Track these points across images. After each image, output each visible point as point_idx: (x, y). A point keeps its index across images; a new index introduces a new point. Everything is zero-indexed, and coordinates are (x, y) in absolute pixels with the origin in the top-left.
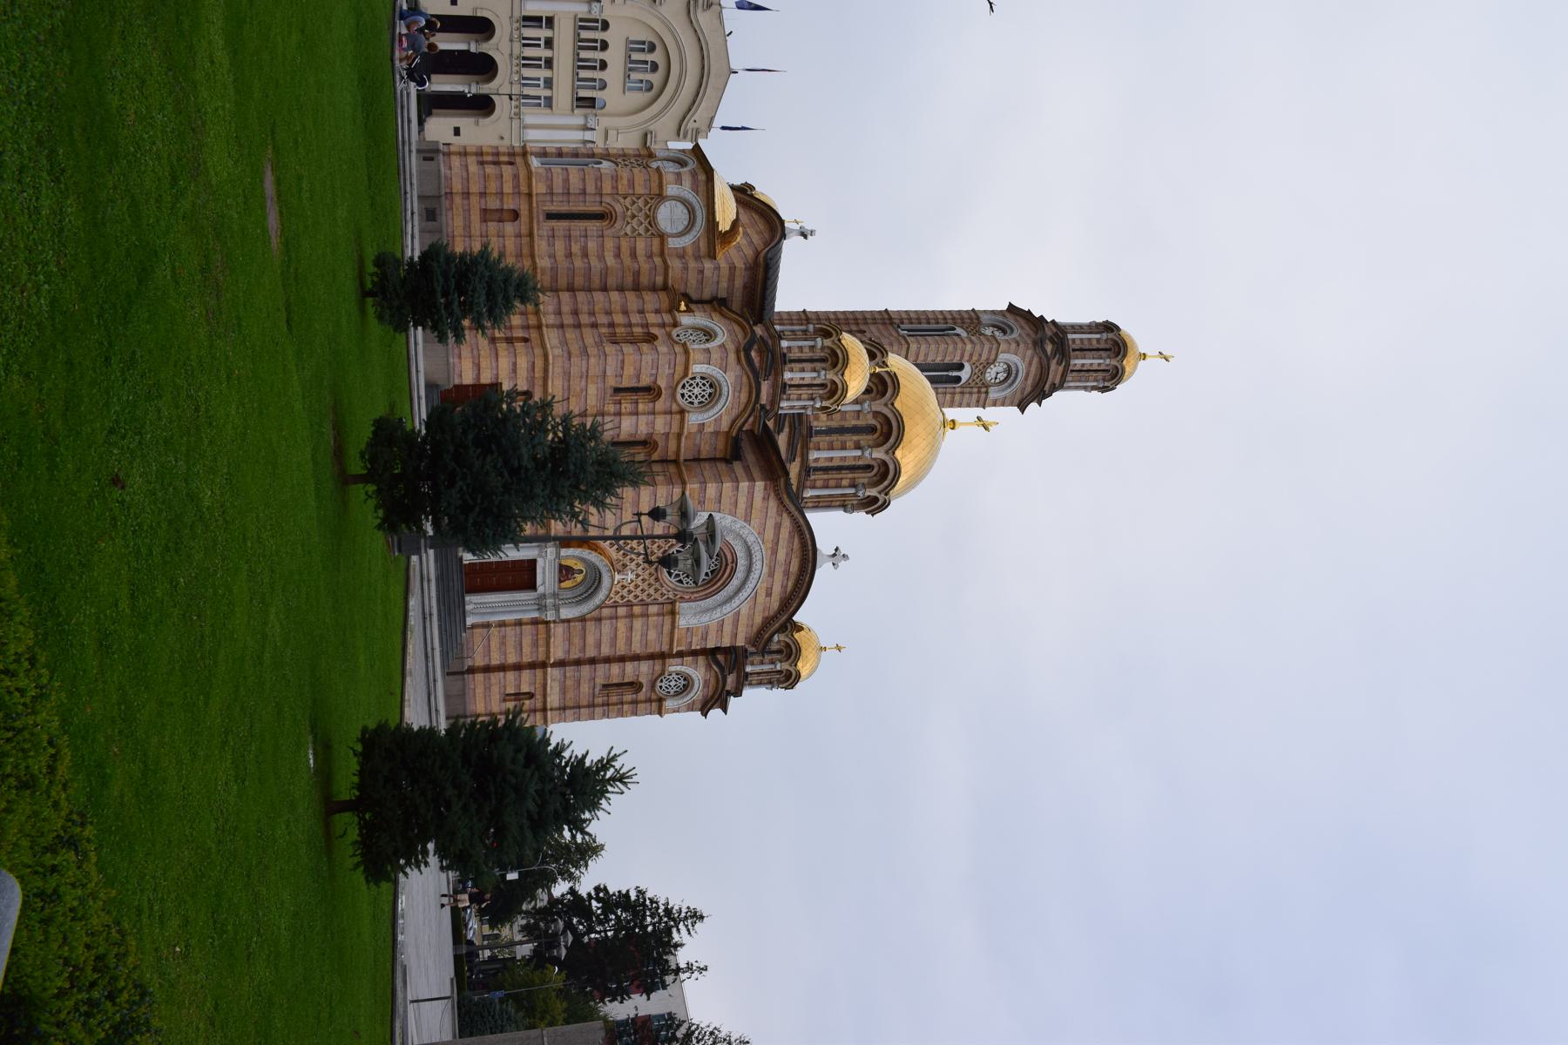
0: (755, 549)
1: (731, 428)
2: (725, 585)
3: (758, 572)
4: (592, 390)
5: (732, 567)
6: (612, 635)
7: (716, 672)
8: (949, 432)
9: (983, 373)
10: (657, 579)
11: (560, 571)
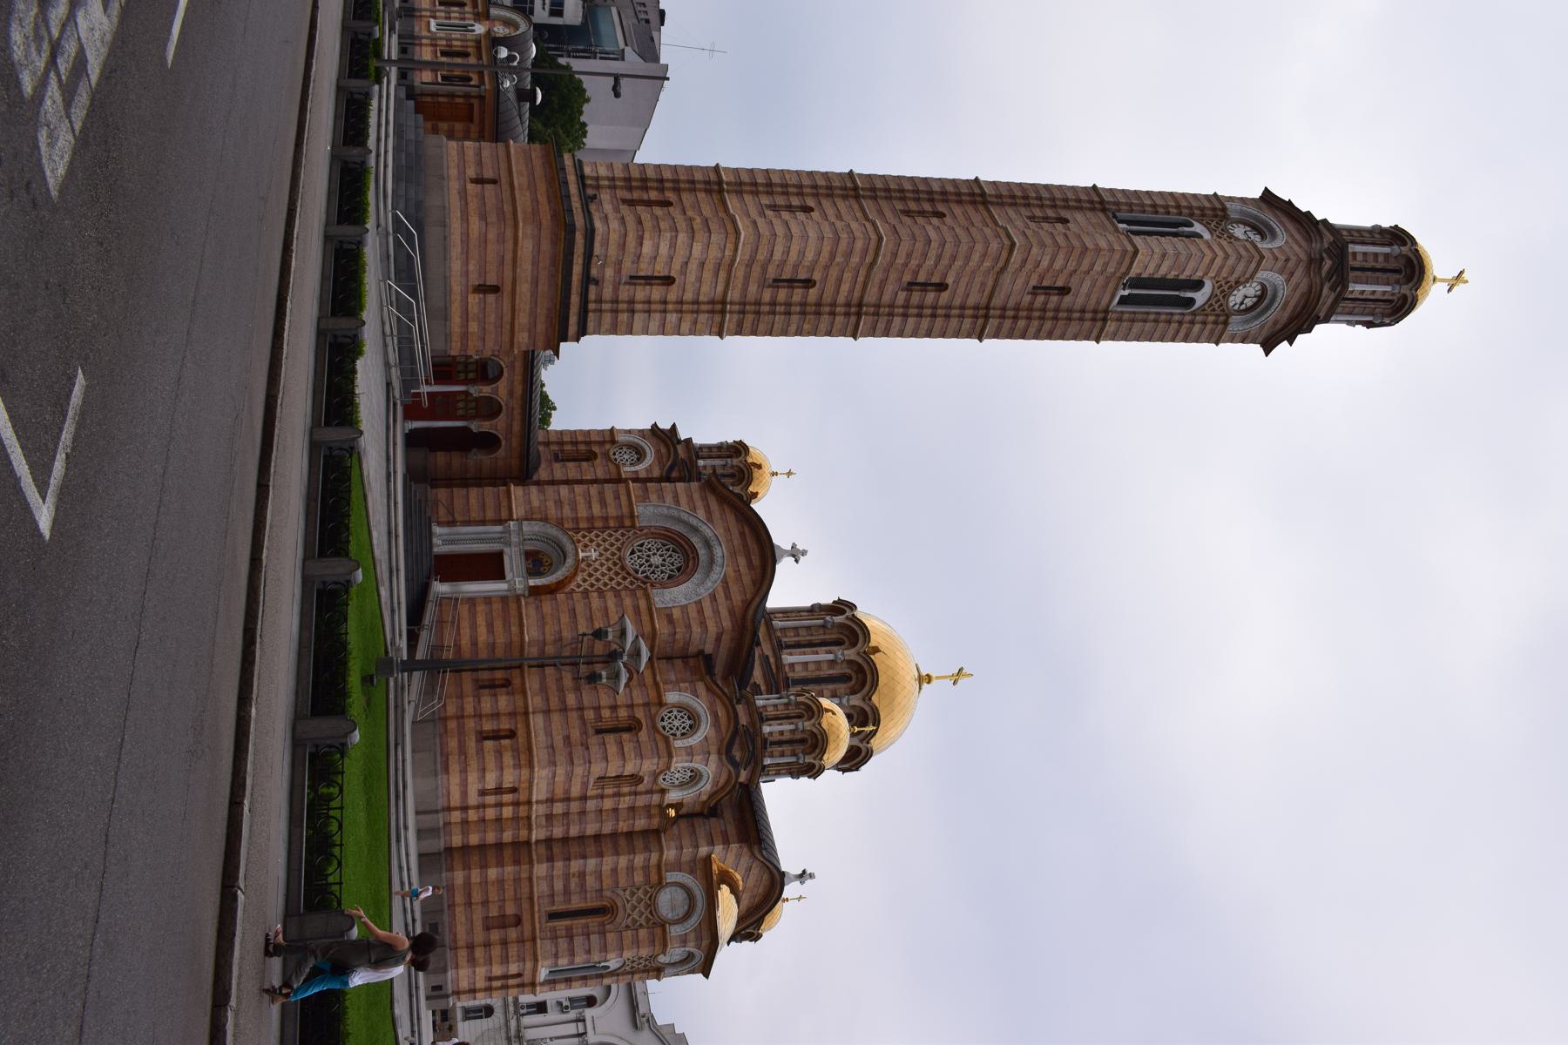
8: (925, 686)
10: (623, 568)
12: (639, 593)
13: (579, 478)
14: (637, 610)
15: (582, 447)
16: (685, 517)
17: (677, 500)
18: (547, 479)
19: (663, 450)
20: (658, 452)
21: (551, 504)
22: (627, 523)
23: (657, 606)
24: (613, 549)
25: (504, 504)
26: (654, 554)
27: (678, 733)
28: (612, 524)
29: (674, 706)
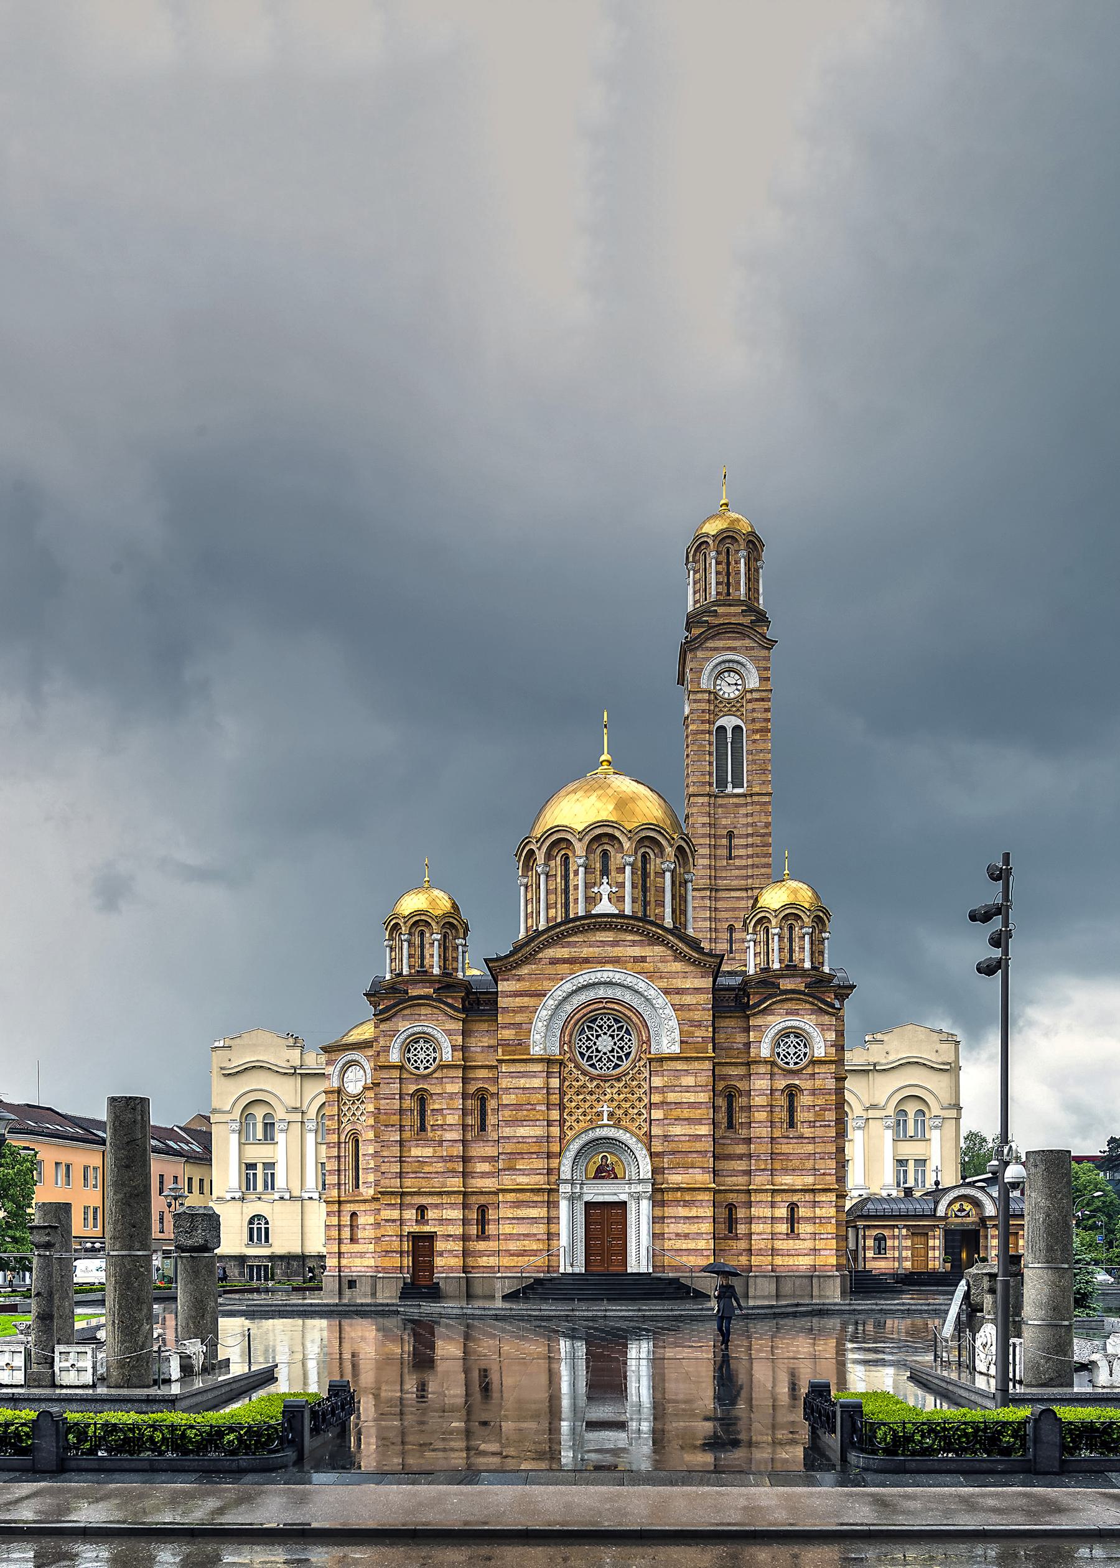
0: (582, 981)
2: (631, 1008)
3: (611, 974)
4: (416, 1152)
7: (774, 1003)
9: (729, 701)
11: (603, 1178)
15: (408, 1103)
24: (591, 1086)
27: (804, 1050)
29: (773, 1050)
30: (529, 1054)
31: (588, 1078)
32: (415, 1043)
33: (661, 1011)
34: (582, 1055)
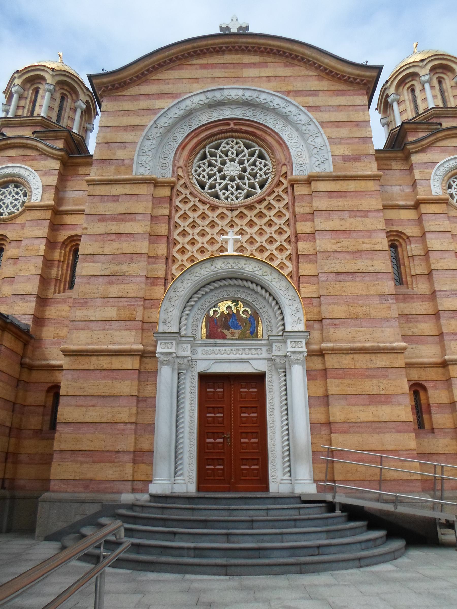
1: (57, 159)
5: (235, 124)
6: (348, 256)
10: (250, 207)
12: (300, 190)
13: (41, 260)
14: (331, 194)
16: (165, 121)
17: (134, 128)
18: (33, 304)
19: (12, 153)
20: (11, 159)
21: (114, 291)
22: (166, 192)
23: (332, 170)
24: (213, 215)
25: (104, 362)
26: (220, 170)
28: (166, 212)
29: (444, 192)
30: (132, 174)
31: (208, 206)
32: (4, 188)
33: (304, 128)
34: (203, 187)
